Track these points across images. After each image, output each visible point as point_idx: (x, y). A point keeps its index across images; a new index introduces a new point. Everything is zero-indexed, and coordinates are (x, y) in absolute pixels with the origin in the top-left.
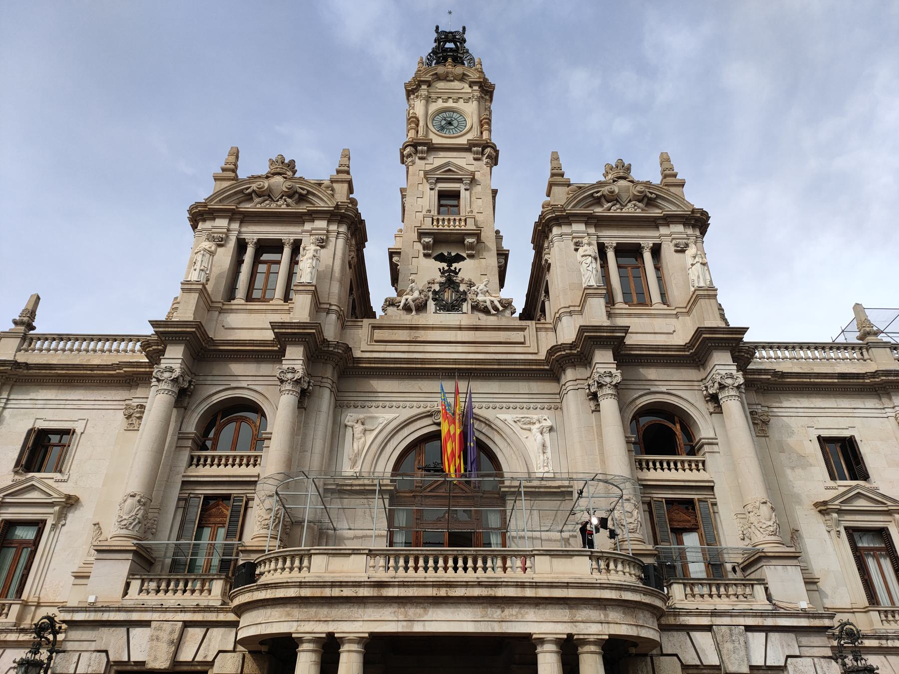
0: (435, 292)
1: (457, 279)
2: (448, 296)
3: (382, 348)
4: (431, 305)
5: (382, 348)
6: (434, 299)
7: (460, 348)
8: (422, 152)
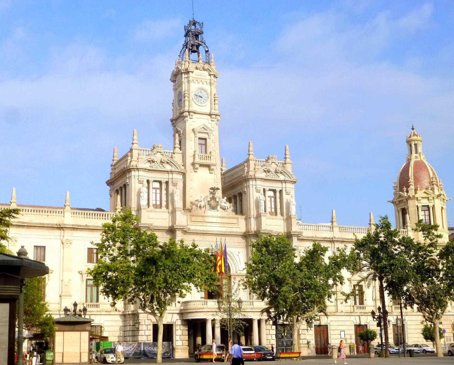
0: (208, 202)
1: (215, 196)
2: (213, 203)
3: (194, 224)
4: (208, 206)
5: (194, 224)
6: (208, 204)
7: (218, 225)
8: (191, 116)
